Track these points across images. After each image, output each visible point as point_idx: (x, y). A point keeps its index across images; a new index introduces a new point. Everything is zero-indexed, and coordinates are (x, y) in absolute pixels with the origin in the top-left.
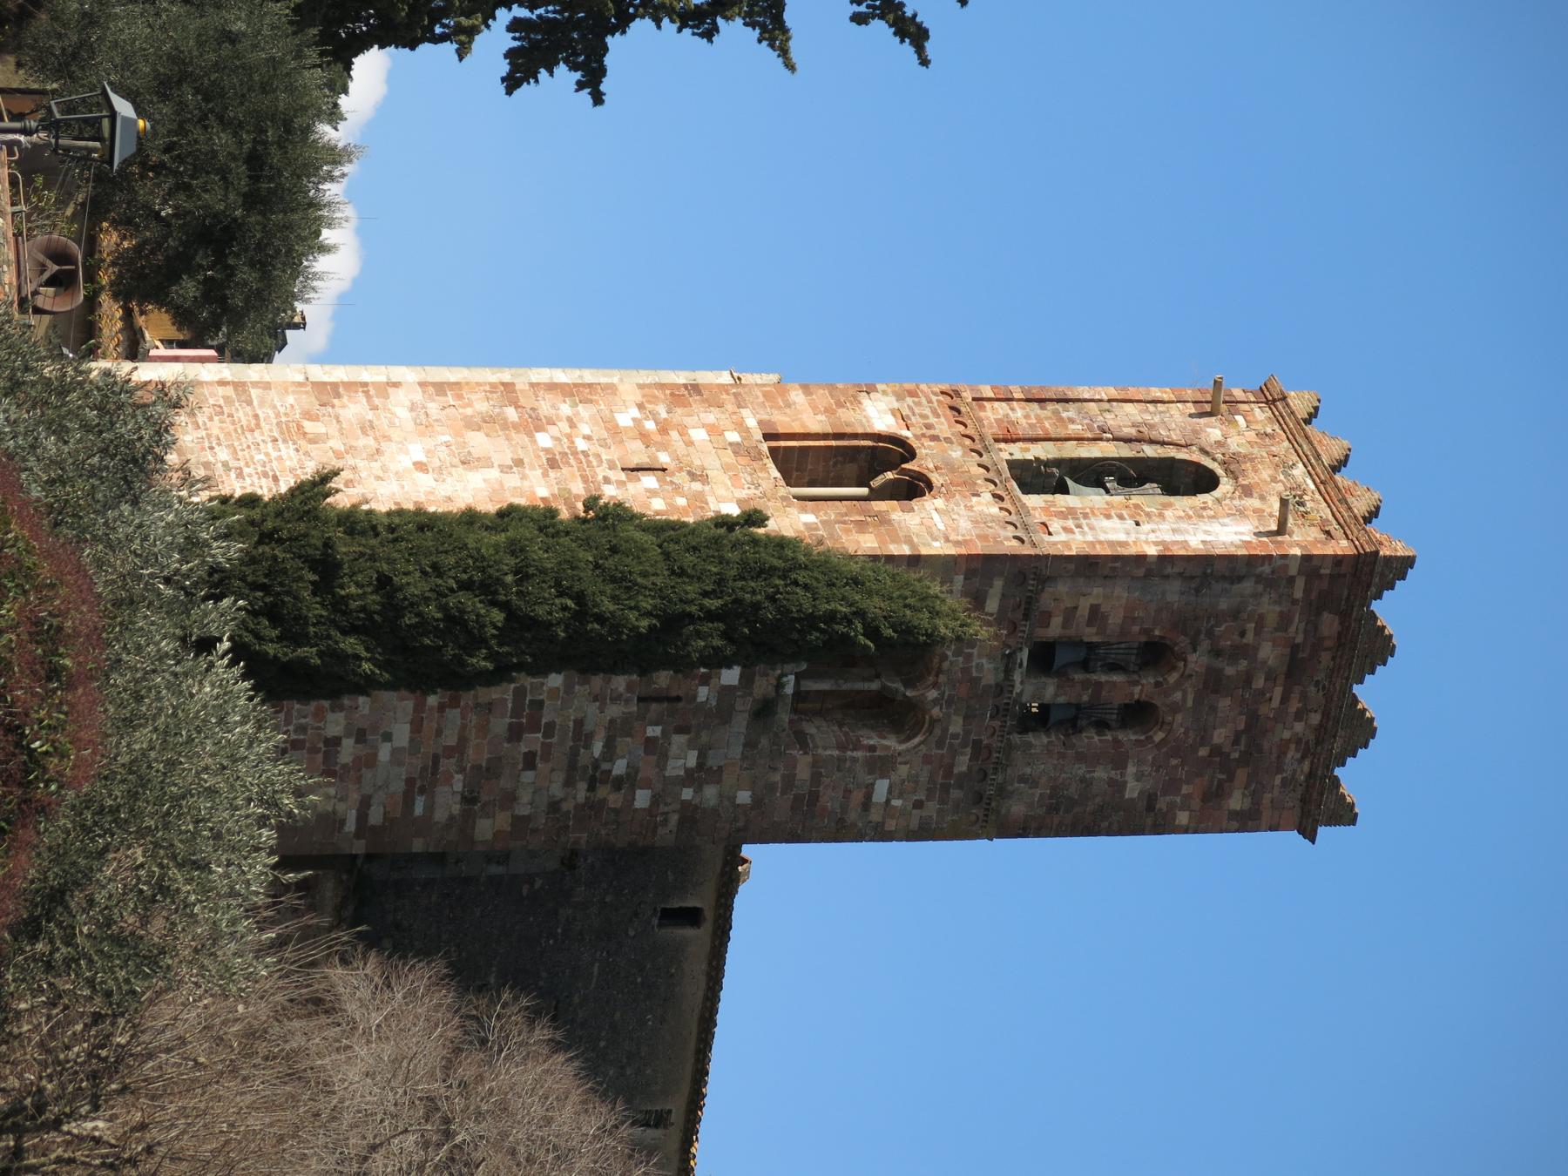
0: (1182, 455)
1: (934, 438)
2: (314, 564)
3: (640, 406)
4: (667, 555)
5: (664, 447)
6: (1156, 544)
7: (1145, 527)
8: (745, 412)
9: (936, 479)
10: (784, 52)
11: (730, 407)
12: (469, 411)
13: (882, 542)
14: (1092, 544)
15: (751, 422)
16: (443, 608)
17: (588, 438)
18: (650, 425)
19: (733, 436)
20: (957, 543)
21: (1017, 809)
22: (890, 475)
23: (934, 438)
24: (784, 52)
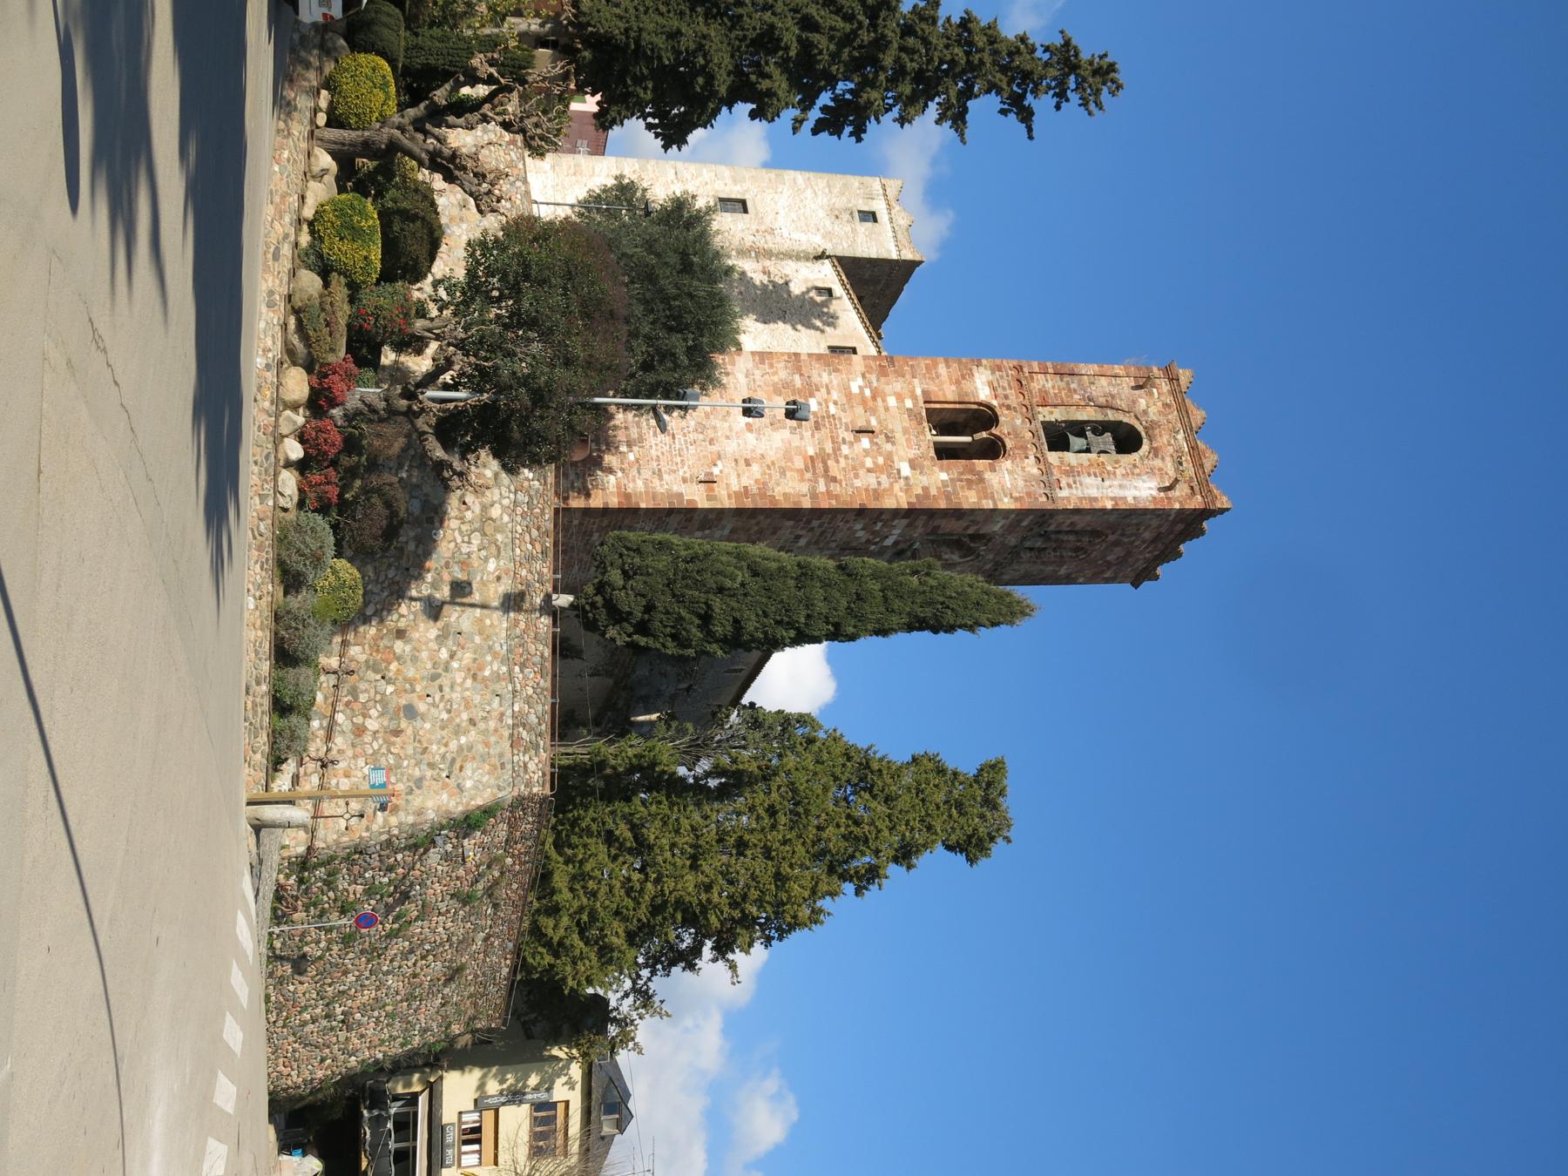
0: (1125, 420)
1: (1008, 407)
2: (699, 616)
3: (864, 376)
4: (885, 598)
5: (874, 411)
6: (1113, 499)
7: (1107, 483)
8: (916, 381)
9: (1009, 444)
10: (962, 135)
11: (908, 376)
12: (776, 379)
13: (980, 499)
14: (1081, 499)
15: (919, 392)
16: (765, 633)
17: (835, 403)
18: (867, 392)
19: (909, 404)
20: (1016, 499)
21: (1006, 577)
22: (984, 435)
23: (1008, 407)
24: (962, 135)
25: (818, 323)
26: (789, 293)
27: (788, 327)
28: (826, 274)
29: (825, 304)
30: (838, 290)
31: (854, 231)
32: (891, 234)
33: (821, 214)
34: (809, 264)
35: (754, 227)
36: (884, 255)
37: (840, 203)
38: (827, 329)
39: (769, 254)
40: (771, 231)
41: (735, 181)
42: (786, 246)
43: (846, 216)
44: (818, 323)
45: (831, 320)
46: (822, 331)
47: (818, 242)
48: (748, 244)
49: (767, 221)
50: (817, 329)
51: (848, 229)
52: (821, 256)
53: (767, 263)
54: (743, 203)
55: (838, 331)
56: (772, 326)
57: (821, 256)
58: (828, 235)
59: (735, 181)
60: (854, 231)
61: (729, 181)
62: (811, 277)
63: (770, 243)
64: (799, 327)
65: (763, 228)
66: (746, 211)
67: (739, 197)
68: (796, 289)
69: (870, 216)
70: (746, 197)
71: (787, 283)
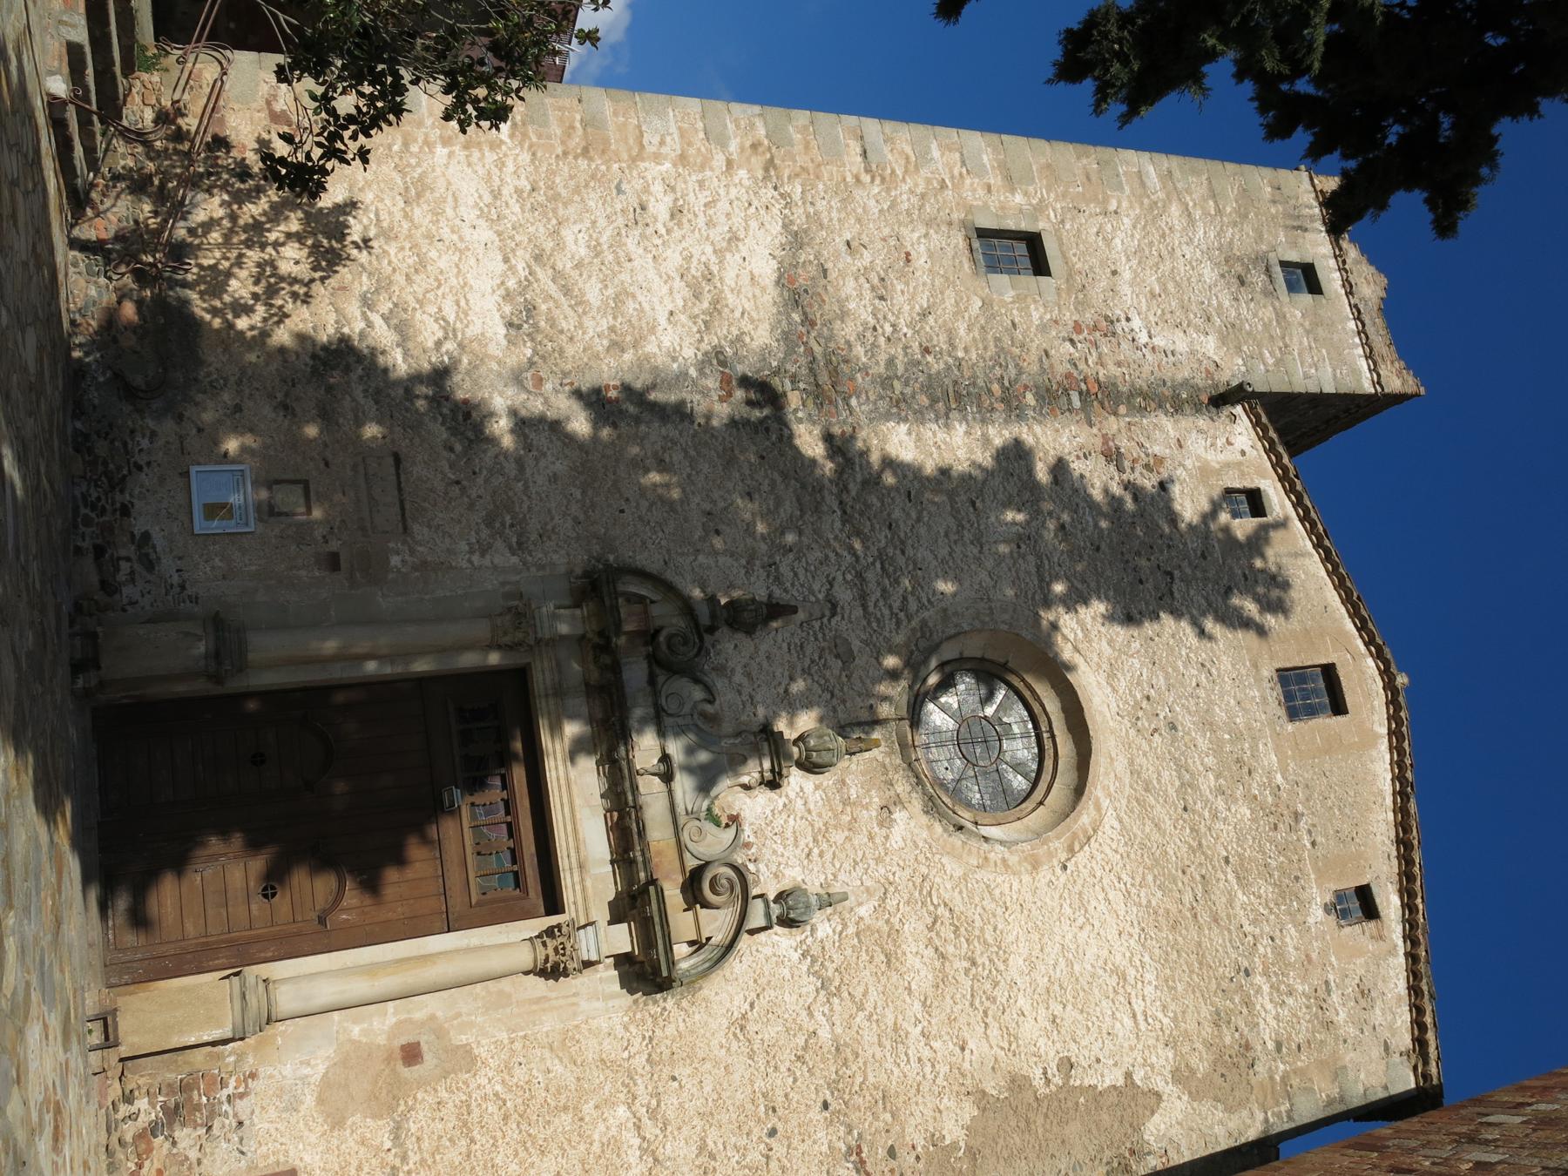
25: (1250, 607)
26: (1173, 518)
27: (1185, 626)
28: (1237, 449)
29: (1257, 543)
30: (1278, 501)
31: (1280, 317)
32: (1352, 325)
33: (1209, 273)
34: (1202, 422)
35: (1069, 317)
36: (1348, 386)
37: (1243, 240)
38: (1271, 620)
39: (1100, 397)
40: (1108, 327)
41: (1010, 182)
42: (1147, 370)
43: (1258, 279)
44: (1250, 607)
45: (1274, 592)
46: (1262, 631)
47: (1205, 353)
48: (1062, 369)
49: (1097, 293)
50: (1246, 623)
51: (1268, 313)
52: (1223, 399)
53: (1112, 424)
54: (1033, 242)
55: (1295, 623)
56: (1149, 628)
57: (1223, 399)
58: (1231, 334)
59: (1010, 182)
60: (1280, 317)
61: (995, 180)
62: (1214, 458)
63: (1108, 364)
64: (1209, 624)
65: (1089, 317)
66: (1040, 266)
67: (1024, 226)
68: (1189, 505)
69: (1306, 278)
70: (1041, 226)
71: (1163, 486)
